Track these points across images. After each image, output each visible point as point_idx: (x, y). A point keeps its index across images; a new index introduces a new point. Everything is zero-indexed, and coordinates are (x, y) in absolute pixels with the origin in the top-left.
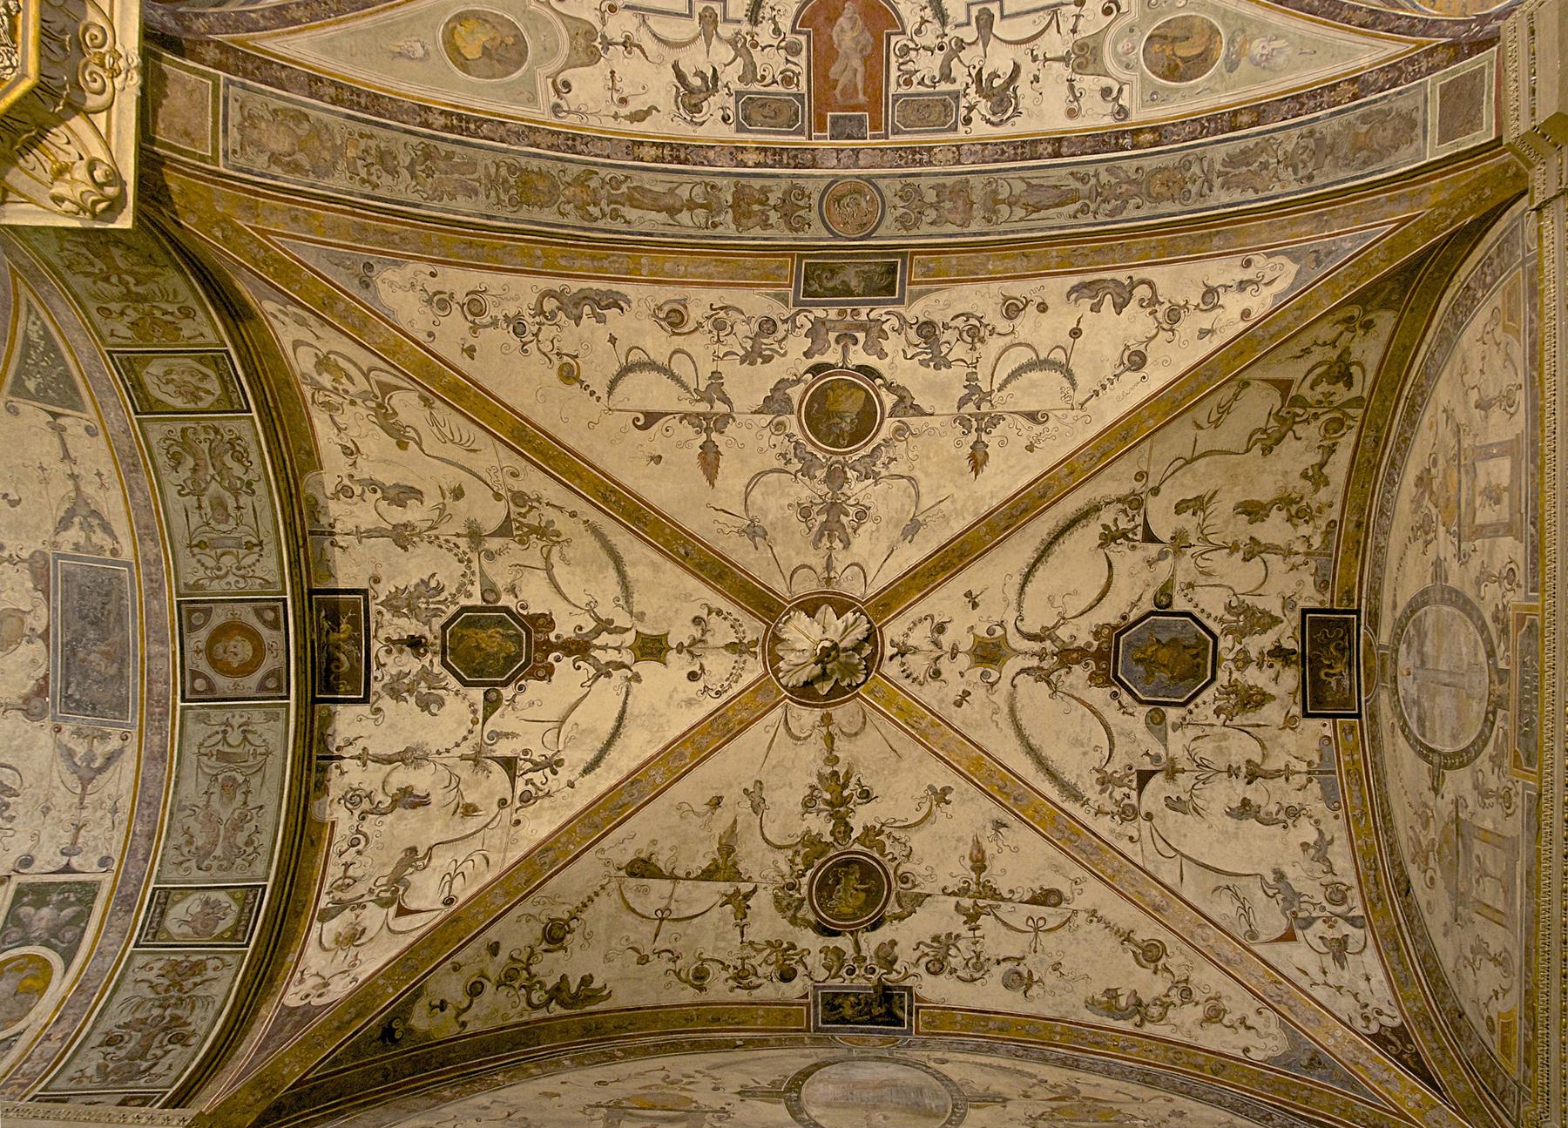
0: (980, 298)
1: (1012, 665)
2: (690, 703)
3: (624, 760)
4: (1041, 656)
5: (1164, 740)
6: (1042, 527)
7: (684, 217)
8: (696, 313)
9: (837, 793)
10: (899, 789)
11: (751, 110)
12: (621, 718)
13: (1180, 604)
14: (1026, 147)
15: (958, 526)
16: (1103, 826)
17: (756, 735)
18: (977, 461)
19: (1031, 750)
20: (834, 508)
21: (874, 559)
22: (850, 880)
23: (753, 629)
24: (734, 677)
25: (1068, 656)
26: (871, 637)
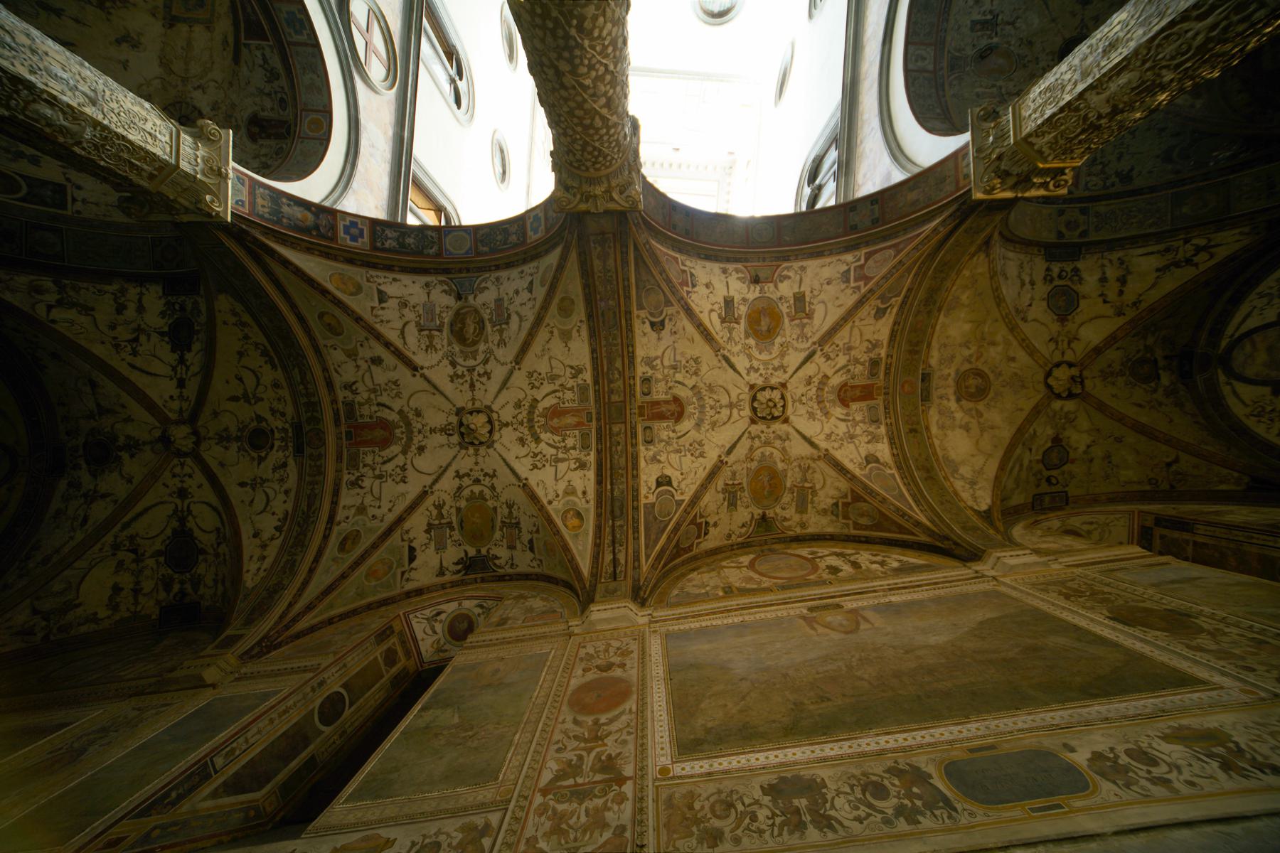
0: (292, 482)
1: (178, 502)
2: (161, 397)
3: (134, 376)
4: (182, 511)
5: (151, 557)
6: (220, 509)
7: (301, 387)
8: (280, 392)
9: (133, 446)
10: (134, 467)
11: (350, 406)
12: (155, 375)
13: (201, 558)
14: (336, 493)
15: (222, 480)
16: (109, 538)
17: (151, 419)
18: (242, 485)
19: (146, 510)
20: (228, 439)
21: (212, 453)
22: (103, 453)
23: (186, 415)
24: (171, 410)
25: (182, 521)
26: (186, 455)
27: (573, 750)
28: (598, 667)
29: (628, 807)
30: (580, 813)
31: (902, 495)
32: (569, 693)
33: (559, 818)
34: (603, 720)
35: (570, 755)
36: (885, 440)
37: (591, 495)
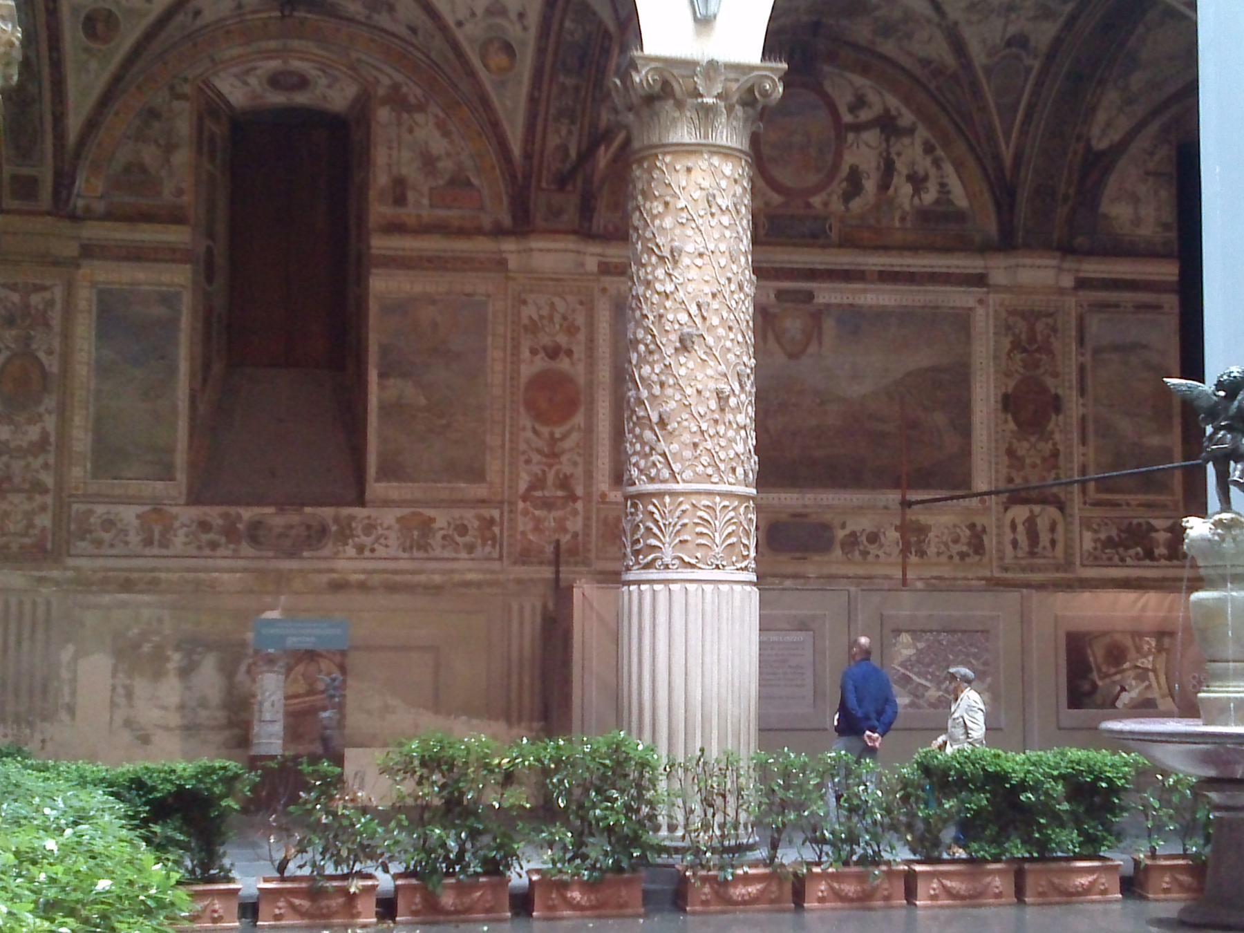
27: (539, 463)
28: (545, 348)
29: (580, 520)
30: (550, 519)
31: (1014, 108)
32: (522, 387)
33: (538, 521)
34: (557, 435)
35: (537, 469)
36: (1062, 20)
37: (533, 19)
